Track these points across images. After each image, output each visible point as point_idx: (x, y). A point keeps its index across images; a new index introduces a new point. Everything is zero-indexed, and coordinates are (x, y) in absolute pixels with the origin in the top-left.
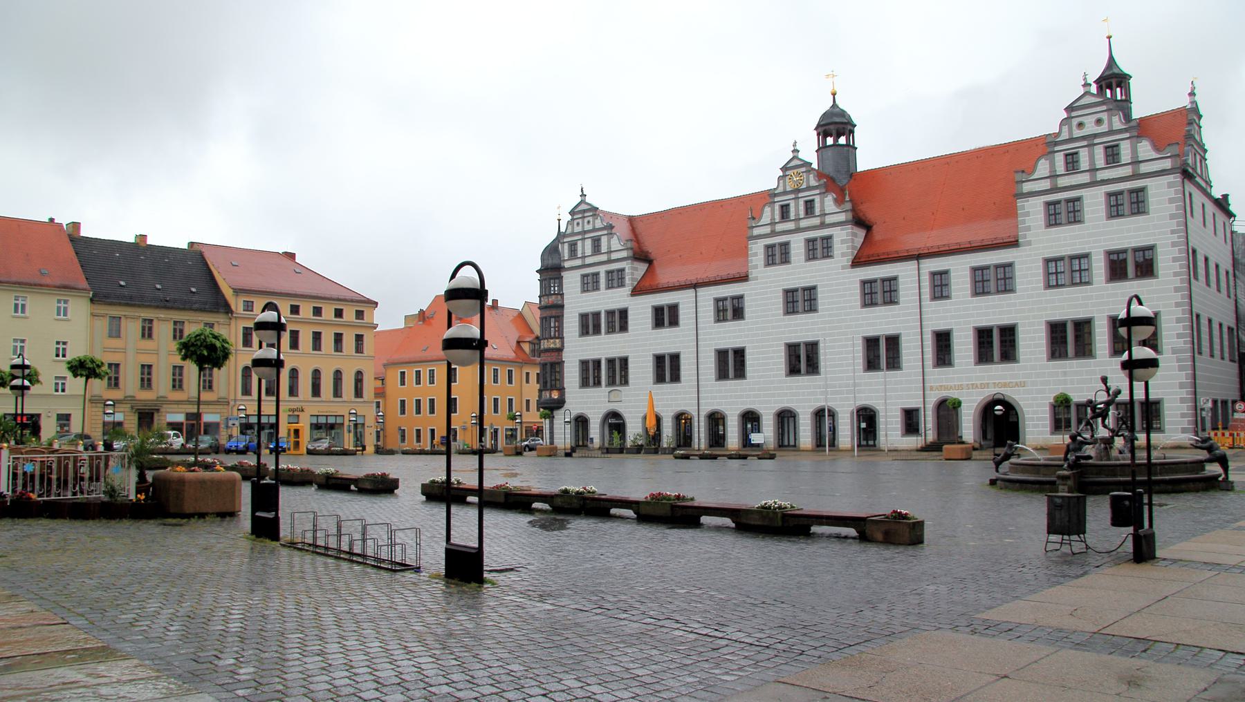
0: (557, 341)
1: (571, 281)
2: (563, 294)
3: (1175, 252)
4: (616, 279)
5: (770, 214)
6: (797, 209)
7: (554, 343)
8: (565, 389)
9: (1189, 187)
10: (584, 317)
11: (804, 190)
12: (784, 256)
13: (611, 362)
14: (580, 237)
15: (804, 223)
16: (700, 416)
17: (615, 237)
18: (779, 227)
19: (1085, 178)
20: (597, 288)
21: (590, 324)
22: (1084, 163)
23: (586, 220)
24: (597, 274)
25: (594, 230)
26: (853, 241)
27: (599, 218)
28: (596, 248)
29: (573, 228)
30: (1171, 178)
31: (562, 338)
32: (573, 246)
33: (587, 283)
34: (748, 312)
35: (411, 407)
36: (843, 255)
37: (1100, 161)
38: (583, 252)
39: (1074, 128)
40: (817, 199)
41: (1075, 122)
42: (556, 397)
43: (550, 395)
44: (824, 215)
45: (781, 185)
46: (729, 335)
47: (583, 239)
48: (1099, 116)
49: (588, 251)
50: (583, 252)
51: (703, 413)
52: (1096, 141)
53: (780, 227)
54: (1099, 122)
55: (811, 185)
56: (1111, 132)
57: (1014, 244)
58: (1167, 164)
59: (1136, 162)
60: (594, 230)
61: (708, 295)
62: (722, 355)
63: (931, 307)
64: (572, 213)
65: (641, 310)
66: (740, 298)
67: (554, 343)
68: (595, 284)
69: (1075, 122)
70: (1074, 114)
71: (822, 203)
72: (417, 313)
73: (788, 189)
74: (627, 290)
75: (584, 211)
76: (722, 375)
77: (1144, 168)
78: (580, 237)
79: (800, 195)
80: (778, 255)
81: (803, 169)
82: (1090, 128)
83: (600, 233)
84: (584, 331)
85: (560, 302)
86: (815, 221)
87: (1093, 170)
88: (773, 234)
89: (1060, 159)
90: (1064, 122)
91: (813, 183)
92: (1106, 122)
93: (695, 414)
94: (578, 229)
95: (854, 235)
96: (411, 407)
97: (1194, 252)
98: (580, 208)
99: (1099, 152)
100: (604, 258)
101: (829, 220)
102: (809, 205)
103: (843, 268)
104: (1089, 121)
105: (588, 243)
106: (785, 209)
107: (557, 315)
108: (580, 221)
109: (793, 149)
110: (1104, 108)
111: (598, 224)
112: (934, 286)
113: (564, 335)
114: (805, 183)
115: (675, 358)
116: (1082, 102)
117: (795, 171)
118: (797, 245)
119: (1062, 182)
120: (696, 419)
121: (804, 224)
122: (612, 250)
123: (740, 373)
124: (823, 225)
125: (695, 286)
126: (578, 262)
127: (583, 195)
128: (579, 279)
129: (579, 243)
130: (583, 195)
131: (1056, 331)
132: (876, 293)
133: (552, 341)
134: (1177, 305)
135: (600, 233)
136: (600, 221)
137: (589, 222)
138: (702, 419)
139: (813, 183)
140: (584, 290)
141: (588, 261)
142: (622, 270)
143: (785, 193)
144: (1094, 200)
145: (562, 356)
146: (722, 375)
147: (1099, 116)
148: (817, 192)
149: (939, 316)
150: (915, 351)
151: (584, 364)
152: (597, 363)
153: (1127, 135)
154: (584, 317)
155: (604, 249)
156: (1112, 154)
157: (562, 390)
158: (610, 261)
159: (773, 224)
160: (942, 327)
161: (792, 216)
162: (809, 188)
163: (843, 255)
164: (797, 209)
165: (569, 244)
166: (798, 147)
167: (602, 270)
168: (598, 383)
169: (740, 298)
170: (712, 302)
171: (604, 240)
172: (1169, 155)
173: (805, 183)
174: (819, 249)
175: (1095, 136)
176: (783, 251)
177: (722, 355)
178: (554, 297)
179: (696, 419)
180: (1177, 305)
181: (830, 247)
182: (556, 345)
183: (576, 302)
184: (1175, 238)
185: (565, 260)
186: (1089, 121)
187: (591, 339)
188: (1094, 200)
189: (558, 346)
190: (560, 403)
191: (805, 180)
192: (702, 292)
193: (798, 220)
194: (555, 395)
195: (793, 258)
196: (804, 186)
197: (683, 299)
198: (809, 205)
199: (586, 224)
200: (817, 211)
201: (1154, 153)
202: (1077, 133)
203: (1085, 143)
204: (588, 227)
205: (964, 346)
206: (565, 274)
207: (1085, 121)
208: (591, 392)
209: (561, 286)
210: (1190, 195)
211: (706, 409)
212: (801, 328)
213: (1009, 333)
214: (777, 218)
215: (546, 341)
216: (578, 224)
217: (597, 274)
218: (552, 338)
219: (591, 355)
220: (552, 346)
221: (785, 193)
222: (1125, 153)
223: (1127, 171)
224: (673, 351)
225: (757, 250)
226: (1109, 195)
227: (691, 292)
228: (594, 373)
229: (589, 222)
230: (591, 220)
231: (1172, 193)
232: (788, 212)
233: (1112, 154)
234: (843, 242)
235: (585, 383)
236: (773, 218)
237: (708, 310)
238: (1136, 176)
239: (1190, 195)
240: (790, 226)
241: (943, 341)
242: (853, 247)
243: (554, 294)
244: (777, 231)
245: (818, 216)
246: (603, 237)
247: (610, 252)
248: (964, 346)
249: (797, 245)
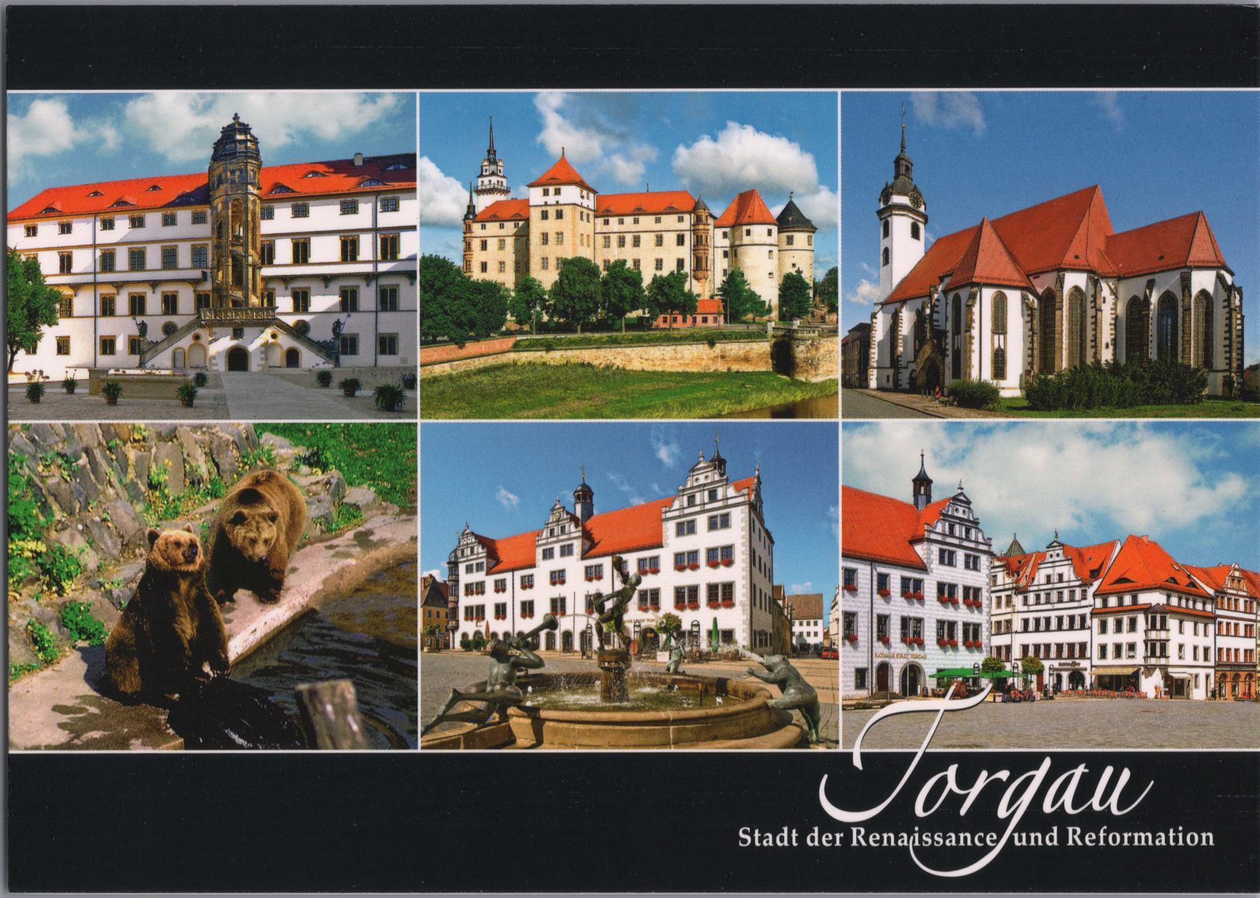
1: (462, 568)
4: (479, 567)
19: (697, 509)
21: (469, 590)
22: (698, 500)
32: (463, 551)
46: (527, 595)
49: (469, 553)
53: (550, 540)
57: (660, 546)
58: (741, 499)
61: (518, 574)
62: (524, 604)
65: (490, 582)
74: (484, 573)
77: (730, 502)
80: (548, 554)
82: (702, 480)
86: (565, 537)
89: (685, 498)
101: (572, 535)
106: (552, 531)
115: (504, 605)
125: (513, 570)
144: (702, 521)
151: (467, 608)
156: (713, 496)
161: (556, 534)
167: (474, 562)
174: (567, 551)
175: (705, 485)
177: (524, 604)
188: (702, 521)
192: (516, 573)
197: (508, 576)
198: (563, 528)
202: (695, 484)
211: (516, 632)
222: (720, 496)
225: (539, 551)
227: (510, 574)
233: (713, 496)
240: (554, 539)
249: (557, 548)
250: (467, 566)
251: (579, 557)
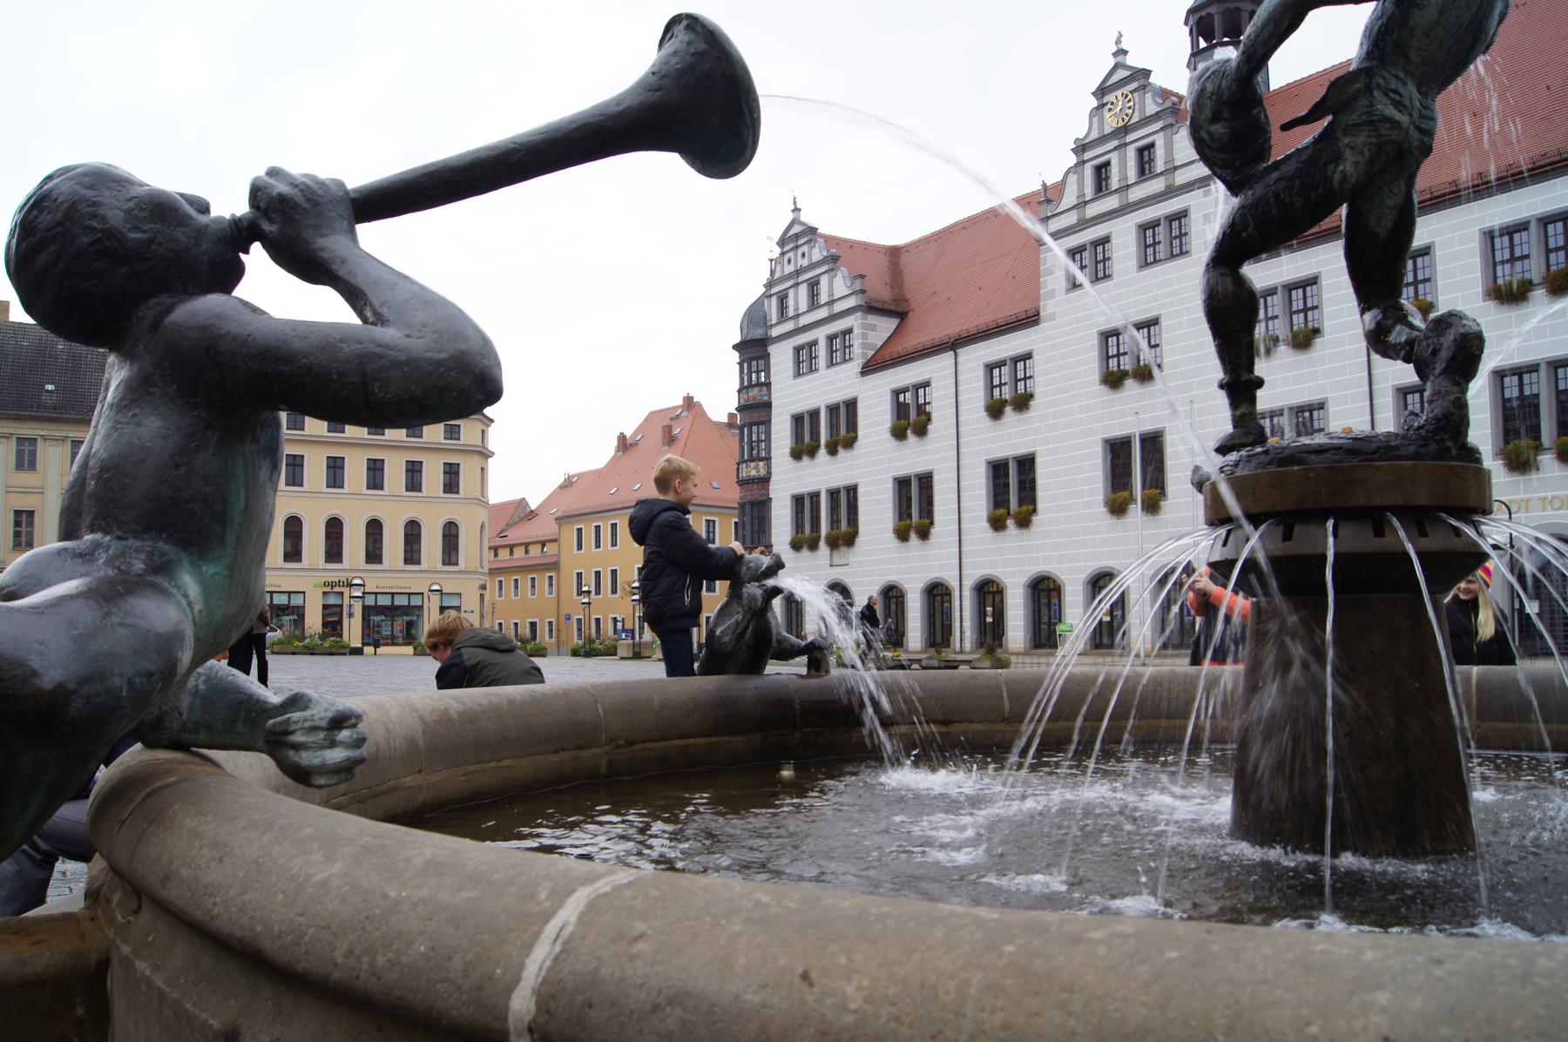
1: (781, 356)
7: (756, 468)
13: (834, 494)
14: (791, 282)
25: (812, 266)
31: (768, 459)
47: (798, 284)
51: (969, 583)
60: (812, 266)
67: (756, 468)
75: (797, 236)
78: (791, 282)
94: (789, 269)
105: (803, 290)
107: (762, 419)
113: (773, 454)
120: (957, 594)
126: (789, 326)
130: (796, 210)
133: (753, 464)
137: (803, 255)
142: (850, 331)
151: (798, 500)
152: (815, 496)
167: (820, 334)
178: (756, 390)
179: (957, 594)
189: (763, 472)
215: (744, 465)
216: (789, 261)
219: (805, 488)
220: (753, 473)
224: (1022, 450)
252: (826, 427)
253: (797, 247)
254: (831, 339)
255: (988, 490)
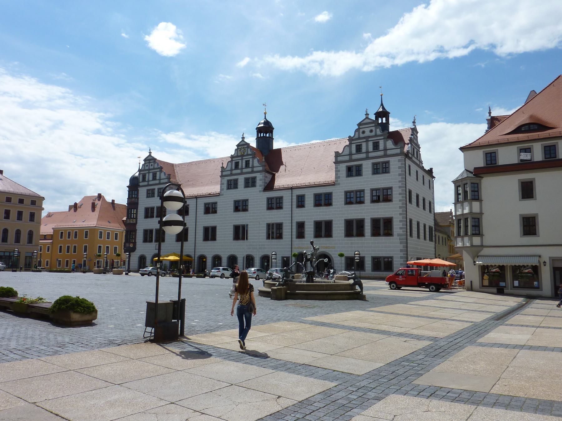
0: (134, 220)
1: (142, 192)
2: (138, 198)
3: (400, 191)
5: (230, 166)
6: (242, 164)
8: (136, 243)
9: (408, 162)
10: (147, 209)
11: (245, 156)
12: (235, 185)
14: (147, 172)
15: (244, 171)
16: (195, 257)
17: (163, 173)
18: (234, 172)
19: (363, 156)
20: (154, 196)
21: (149, 213)
23: (151, 164)
24: (154, 189)
25: (154, 169)
26: (265, 180)
27: (156, 163)
28: (154, 178)
29: (145, 167)
30: (399, 158)
31: (136, 218)
33: (150, 194)
34: (219, 210)
35: (65, 249)
36: (260, 186)
37: (371, 148)
38: (148, 179)
39: (361, 133)
40: (251, 160)
41: (361, 130)
42: (132, 246)
43: (129, 245)
44: (253, 167)
45: (236, 153)
47: (149, 173)
48: (371, 128)
49: (151, 178)
50: (148, 179)
52: (370, 139)
53: (234, 172)
54: (371, 131)
55: (249, 153)
56: (376, 136)
59: (385, 150)
60: (154, 169)
62: (206, 229)
63: (297, 211)
64: (145, 160)
66: (216, 203)
67: (133, 221)
68: (153, 194)
69: (361, 130)
70: (361, 127)
71: (253, 162)
72: (73, 204)
73: (239, 154)
75: (150, 160)
76: (206, 238)
77: (389, 152)
78: (147, 172)
79: (244, 158)
81: (246, 146)
82: (368, 133)
83: (156, 170)
84: (146, 217)
85: (136, 202)
86: (249, 170)
87: (367, 152)
88: (232, 175)
90: (357, 131)
91: (249, 152)
92: (374, 131)
93: (193, 256)
95: (266, 177)
96: (65, 249)
97: (410, 192)
98: (148, 158)
99: (371, 144)
100: (157, 182)
101: (255, 169)
102: (247, 163)
103: (260, 191)
104: (367, 131)
105: (151, 175)
108: (148, 164)
109: (242, 137)
110: (373, 125)
111: (156, 166)
112: (298, 201)
114: (246, 153)
116: (365, 122)
117: (242, 147)
118: (241, 180)
119: (354, 157)
121: (244, 171)
122: (161, 178)
123: (214, 238)
124: (253, 172)
126: (146, 183)
127: (150, 153)
128: (146, 191)
129: (147, 175)
131: (349, 224)
132: (274, 204)
133: (131, 220)
134: (400, 214)
135: (156, 170)
136: (157, 165)
137: (152, 165)
138: (196, 258)
139: (249, 152)
140: (148, 197)
141: (151, 183)
143: (237, 156)
144: (367, 166)
145: (136, 227)
146: (206, 238)
147: (371, 128)
148: (251, 157)
149: (300, 215)
150: (288, 231)
151: (146, 231)
153: (382, 137)
154: (147, 209)
155: (158, 178)
156: (376, 146)
157: (135, 244)
158: (160, 184)
159: (231, 170)
160: (300, 220)
162: (248, 155)
163: (260, 186)
164: (242, 164)
165: (142, 175)
166: (244, 136)
167: (156, 187)
168: (151, 241)
169: (216, 203)
170: (203, 205)
171: (158, 174)
172: (399, 147)
173: (246, 153)
174: (250, 183)
175: (369, 137)
176: (235, 183)
177: (206, 229)
180: (400, 214)
181: (255, 182)
182: (133, 222)
183: (144, 202)
184: (400, 184)
185: (140, 182)
186: (367, 131)
187: (149, 220)
188: (367, 166)
189: (134, 222)
190: (133, 249)
191: (246, 151)
193: (242, 169)
194: (131, 246)
195: (239, 186)
196: (246, 154)
198: (247, 163)
199: (150, 166)
200: (251, 165)
201: (393, 146)
202: (362, 135)
203: (365, 140)
204: (151, 167)
205: (309, 230)
206: (140, 189)
207: (366, 131)
208: (148, 244)
209: (138, 194)
210: (409, 166)
211: (198, 254)
212: (241, 218)
213: (329, 225)
214: (233, 167)
215: (129, 220)
217: (154, 189)
218: (132, 218)
220: (131, 222)
221: (237, 156)
222: (381, 147)
223: (381, 153)
226: (374, 164)
228: (150, 236)
229: (152, 165)
230: (153, 164)
231: (399, 164)
232: (238, 165)
233: (376, 146)
234: (260, 180)
235: (145, 241)
236: (232, 168)
237: (201, 209)
238: (386, 156)
239: (409, 166)
240: (238, 171)
241: (301, 226)
242: (265, 183)
243: (135, 198)
244: (233, 173)
245: (251, 168)
246: (157, 172)
247: (160, 179)
248: (309, 230)
249: (241, 180)
250: (148, 190)
251: (261, 188)
252: (156, 212)
253: (150, 163)
254: (159, 189)
255: (203, 234)
